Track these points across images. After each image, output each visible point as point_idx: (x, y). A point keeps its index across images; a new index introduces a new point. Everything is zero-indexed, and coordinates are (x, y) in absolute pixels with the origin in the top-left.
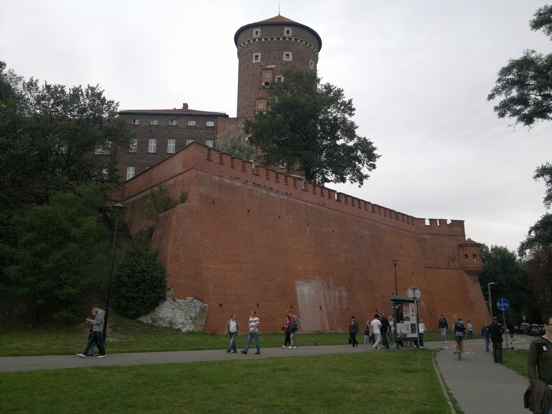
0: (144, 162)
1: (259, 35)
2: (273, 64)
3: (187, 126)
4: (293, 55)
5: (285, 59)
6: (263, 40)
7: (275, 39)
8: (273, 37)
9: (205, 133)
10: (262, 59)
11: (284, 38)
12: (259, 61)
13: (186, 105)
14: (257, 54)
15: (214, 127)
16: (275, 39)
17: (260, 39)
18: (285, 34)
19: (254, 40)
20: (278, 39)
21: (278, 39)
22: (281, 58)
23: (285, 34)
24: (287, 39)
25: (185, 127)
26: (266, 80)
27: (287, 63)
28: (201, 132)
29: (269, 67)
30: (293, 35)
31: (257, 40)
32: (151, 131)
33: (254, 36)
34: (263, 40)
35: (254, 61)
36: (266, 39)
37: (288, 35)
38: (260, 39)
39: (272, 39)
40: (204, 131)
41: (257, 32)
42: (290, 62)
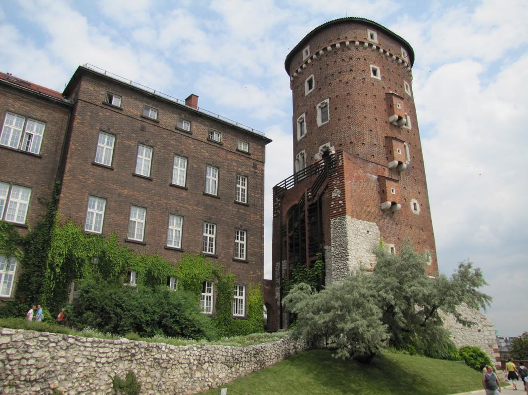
0: (126, 192)
3: (210, 140)
6: (381, 50)
7: (394, 57)
8: (392, 53)
9: (237, 162)
10: (383, 77)
13: (191, 99)
15: (248, 154)
16: (394, 57)
17: (378, 48)
19: (370, 45)
25: (205, 139)
28: (230, 156)
31: (374, 47)
32: (143, 129)
34: (381, 50)
36: (385, 52)
38: (378, 48)
39: (391, 55)
40: (234, 158)
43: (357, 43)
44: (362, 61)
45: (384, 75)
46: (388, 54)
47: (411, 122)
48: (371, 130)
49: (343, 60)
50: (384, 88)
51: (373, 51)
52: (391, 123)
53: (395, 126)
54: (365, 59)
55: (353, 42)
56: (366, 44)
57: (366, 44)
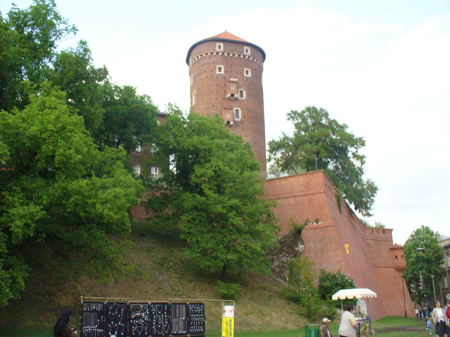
1: (222, 49)
2: (236, 78)
4: (252, 72)
5: (245, 75)
6: (226, 54)
7: (237, 56)
8: (234, 53)
10: (226, 72)
11: (245, 56)
12: (223, 72)
14: (220, 66)
16: (237, 56)
17: (223, 53)
18: (245, 52)
19: (217, 53)
20: (239, 55)
21: (239, 55)
22: (242, 73)
23: (245, 52)
24: (247, 57)
26: (231, 92)
27: (247, 78)
29: (232, 79)
30: (251, 55)
31: (220, 54)
33: (217, 49)
34: (226, 54)
35: (218, 72)
37: (247, 53)
38: (223, 53)
41: (220, 47)
42: (250, 78)
43: (209, 54)
44: (212, 64)
45: (226, 70)
46: (231, 55)
47: (246, 94)
48: (213, 106)
49: (202, 66)
50: (225, 78)
51: (220, 56)
52: (229, 98)
53: (231, 100)
54: (214, 63)
55: (206, 54)
56: (215, 54)
57: (215, 54)
